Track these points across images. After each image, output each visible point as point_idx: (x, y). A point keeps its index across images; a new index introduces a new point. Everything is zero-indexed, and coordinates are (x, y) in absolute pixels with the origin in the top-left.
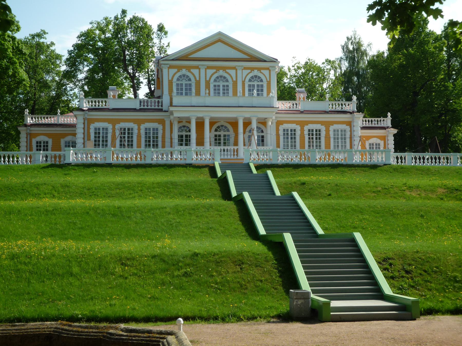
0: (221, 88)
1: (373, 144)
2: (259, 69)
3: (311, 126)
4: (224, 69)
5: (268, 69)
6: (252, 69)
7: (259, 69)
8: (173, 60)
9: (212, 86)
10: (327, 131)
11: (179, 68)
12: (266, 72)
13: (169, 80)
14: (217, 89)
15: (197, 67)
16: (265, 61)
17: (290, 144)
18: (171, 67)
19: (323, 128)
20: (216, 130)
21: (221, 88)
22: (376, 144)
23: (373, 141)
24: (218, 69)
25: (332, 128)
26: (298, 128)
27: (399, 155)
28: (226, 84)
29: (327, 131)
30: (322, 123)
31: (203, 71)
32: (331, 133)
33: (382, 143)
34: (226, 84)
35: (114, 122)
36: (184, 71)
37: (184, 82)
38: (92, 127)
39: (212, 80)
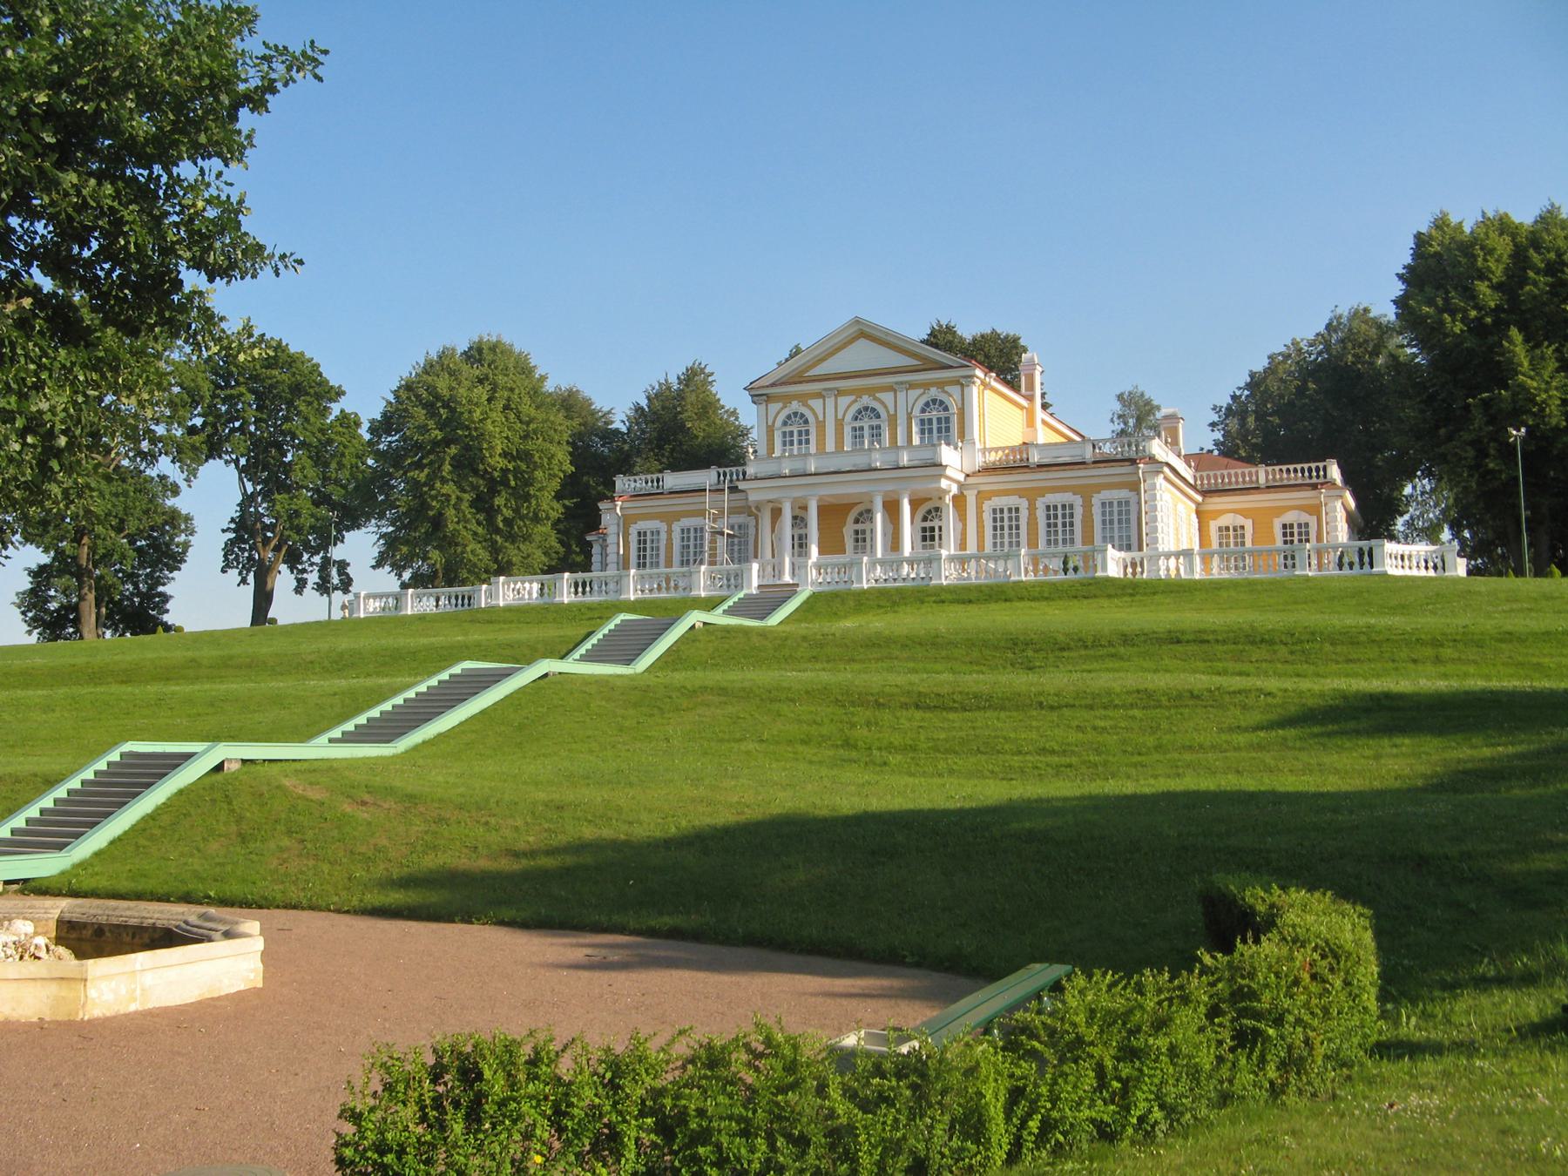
0: (866, 432)
1: (1291, 526)
3: (1052, 498)
4: (871, 391)
5: (957, 382)
7: (940, 385)
8: (773, 385)
9: (847, 430)
10: (1087, 506)
11: (786, 399)
12: (955, 390)
14: (858, 433)
15: (819, 395)
19: (1078, 501)
20: (857, 521)
21: (866, 432)
22: (1300, 526)
23: (1291, 517)
28: (875, 422)
29: (1087, 506)
32: (1097, 511)
33: (1313, 521)
34: (875, 422)
35: (670, 518)
36: (795, 406)
38: (633, 530)
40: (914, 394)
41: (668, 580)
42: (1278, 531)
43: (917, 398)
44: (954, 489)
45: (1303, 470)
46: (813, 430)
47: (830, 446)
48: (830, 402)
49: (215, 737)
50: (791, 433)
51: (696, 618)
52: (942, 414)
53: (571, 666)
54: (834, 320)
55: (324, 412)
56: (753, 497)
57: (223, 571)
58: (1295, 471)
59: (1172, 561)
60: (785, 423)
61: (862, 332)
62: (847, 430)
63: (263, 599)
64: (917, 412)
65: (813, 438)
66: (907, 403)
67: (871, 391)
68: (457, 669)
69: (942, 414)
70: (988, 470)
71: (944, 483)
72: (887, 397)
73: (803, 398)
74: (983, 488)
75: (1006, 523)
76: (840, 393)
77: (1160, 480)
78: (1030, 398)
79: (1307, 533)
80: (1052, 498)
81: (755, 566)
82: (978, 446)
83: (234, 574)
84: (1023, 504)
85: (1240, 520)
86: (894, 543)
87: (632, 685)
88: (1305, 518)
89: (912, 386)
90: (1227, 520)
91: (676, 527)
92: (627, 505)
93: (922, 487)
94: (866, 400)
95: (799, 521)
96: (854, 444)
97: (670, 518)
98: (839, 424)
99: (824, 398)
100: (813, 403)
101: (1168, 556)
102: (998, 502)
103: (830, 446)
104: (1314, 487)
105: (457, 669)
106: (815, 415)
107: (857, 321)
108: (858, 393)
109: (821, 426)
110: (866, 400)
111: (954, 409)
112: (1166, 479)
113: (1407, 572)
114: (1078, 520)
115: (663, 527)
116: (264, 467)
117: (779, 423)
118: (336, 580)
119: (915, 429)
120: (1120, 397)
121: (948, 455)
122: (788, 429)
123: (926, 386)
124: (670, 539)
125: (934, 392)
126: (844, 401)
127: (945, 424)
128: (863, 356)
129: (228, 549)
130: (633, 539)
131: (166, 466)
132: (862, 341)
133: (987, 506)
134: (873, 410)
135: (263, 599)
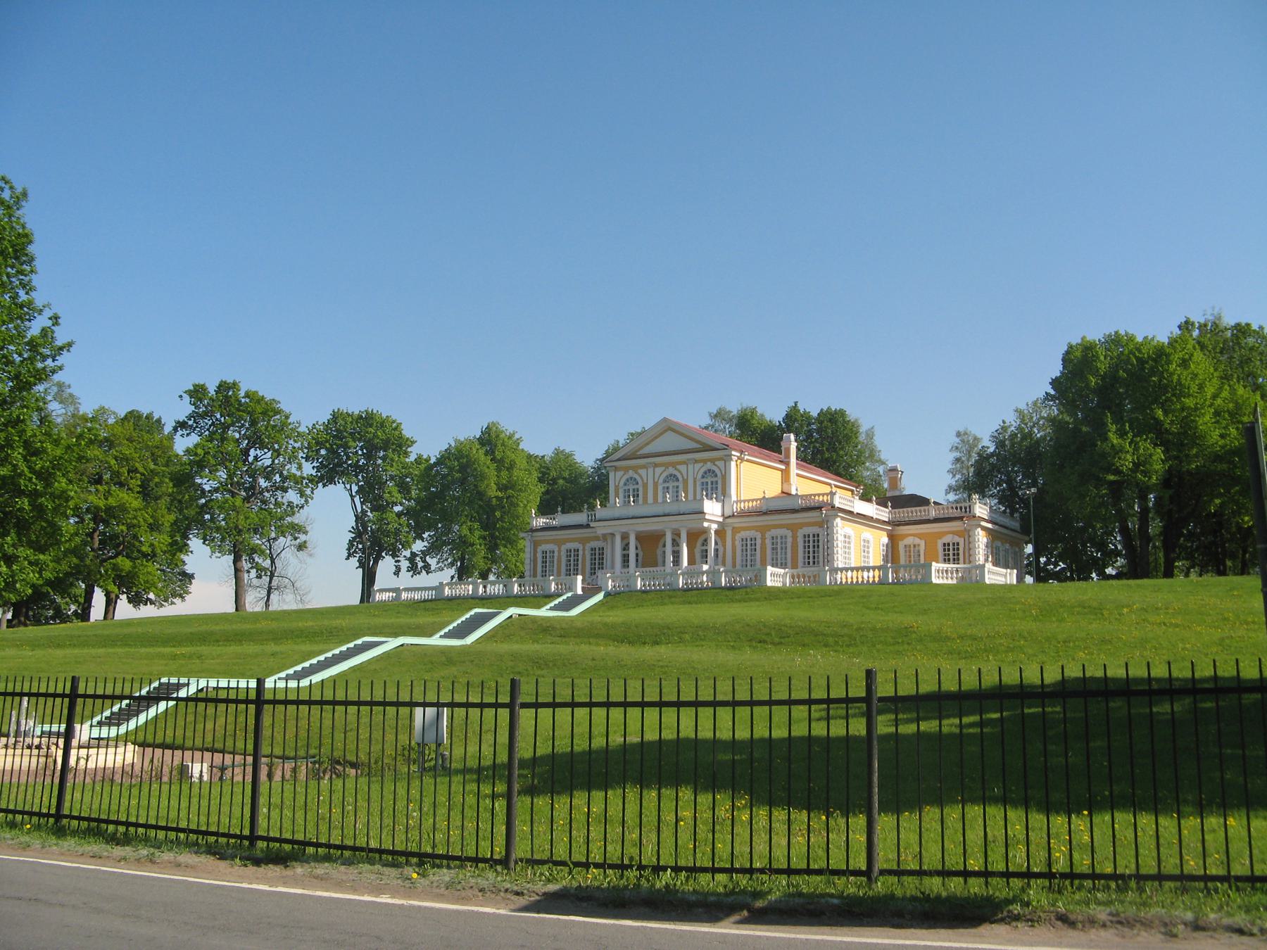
2: (713, 461)
4: (674, 465)
6: (705, 461)
7: (713, 461)
8: (619, 460)
9: (660, 488)
10: (795, 537)
11: (626, 469)
12: (720, 464)
18: (616, 469)
24: (666, 465)
25: (800, 533)
26: (789, 533)
28: (676, 484)
29: (795, 537)
30: (787, 527)
31: (650, 471)
35: (559, 543)
36: (631, 473)
37: (631, 487)
38: (540, 549)
39: (661, 481)
40: (698, 466)
42: (940, 548)
43: (700, 469)
44: (714, 526)
47: (650, 500)
48: (650, 471)
49: (199, 674)
51: (513, 611)
53: (436, 641)
55: (406, 454)
56: (600, 532)
57: (347, 559)
59: (849, 573)
61: (667, 427)
63: (369, 578)
66: (692, 471)
68: (359, 642)
70: (744, 514)
71: (706, 524)
72: (683, 468)
76: (656, 465)
77: (838, 520)
78: (787, 464)
80: (774, 532)
81: (580, 578)
82: (734, 498)
83: (354, 561)
84: (758, 535)
85: (917, 541)
86: (677, 561)
87: (463, 650)
89: (696, 461)
90: (909, 541)
91: (564, 548)
93: (694, 525)
94: (671, 470)
95: (626, 547)
97: (559, 543)
98: (656, 485)
100: (640, 471)
101: (842, 570)
102: (744, 534)
103: (650, 500)
104: (961, 518)
105: (359, 642)
107: (665, 420)
108: (666, 465)
110: (671, 470)
112: (843, 519)
113: (945, 581)
114: (789, 545)
116: (371, 492)
118: (420, 564)
120: (958, 434)
121: (712, 509)
123: (705, 461)
127: (717, 485)
128: (670, 442)
129: (351, 543)
131: (292, 496)
132: (669, 434)
133: (738, 536)
135: (369, 578)
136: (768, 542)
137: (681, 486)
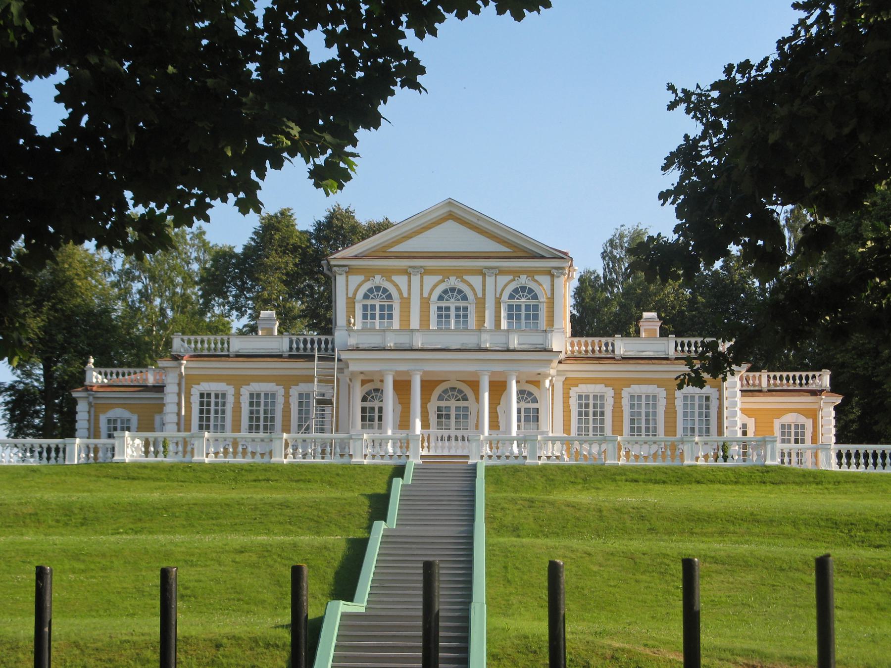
0: (453, 313)
5: (549, 273)
8: (356, 257)
9: (433, 309)
11: (369, 273)
12: (545, 280)
13: (348, 298)
14: (443, 314)
15: (405, 272)
16: (543, 257)
17: (591, 425)
18: (350, 271)
20: (440, 398)
21: (453, 313)
23: (790, 418)
27: (844, 448)
28: (462, 304)
31: (416, 280)
33: (809, 424)
34: (462, 304)
35: (238, 381)
38: (196, 391)
40: (503, 280)
41: (235, 444)
45: (794, 378)
46: (472, 309)
47: (415, 323)
50: (373, 307)
52: (532, 302)
54: (426, 199)
58: (781, 378)
60: (366, 297)
61: (453, 214)
62: (433, 309)
64: (505, 297)
65: (396, 313)
67: (459, 273)
69: (532, 302)
73: (387, 273)
74: (570, 375)
75: (212, 408)
76: (427, 272)
79: (803, 434)
84: (609, 393)
88: (802, 420)
89: (502, 272)
91: (245, 391)
92: (191, 365)
94: (453, 282)
96: (439, 323)
97: (238, 381)
98: (425, 303)
99: (409, 275)
100: (395, 278)
102: (584, 389)
103: (415, 323)
106: (399, 290)
107: (450, 203)
108: (446, 273)
109: (406, 303)
111: (542, 299)
115: (230, 390)
117: (360, 295)
119: (503, 314)
122: (369, 302)
123: (516, 273)
124: (287, 404)
125: (523, 280)
126: (430, 280)
130: (195, 400)
132: (450, 224)
133: (574, 392)
134: (385, 290)
136: (626, 402)
137: (472, 309)
